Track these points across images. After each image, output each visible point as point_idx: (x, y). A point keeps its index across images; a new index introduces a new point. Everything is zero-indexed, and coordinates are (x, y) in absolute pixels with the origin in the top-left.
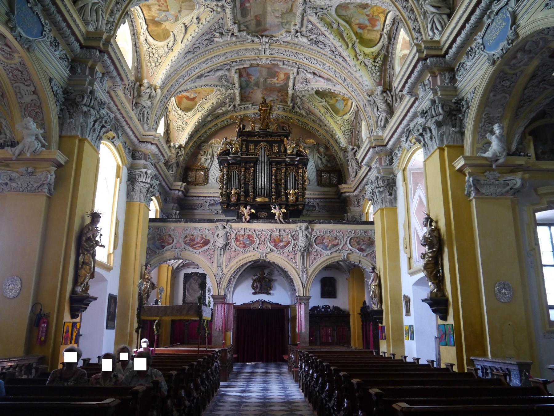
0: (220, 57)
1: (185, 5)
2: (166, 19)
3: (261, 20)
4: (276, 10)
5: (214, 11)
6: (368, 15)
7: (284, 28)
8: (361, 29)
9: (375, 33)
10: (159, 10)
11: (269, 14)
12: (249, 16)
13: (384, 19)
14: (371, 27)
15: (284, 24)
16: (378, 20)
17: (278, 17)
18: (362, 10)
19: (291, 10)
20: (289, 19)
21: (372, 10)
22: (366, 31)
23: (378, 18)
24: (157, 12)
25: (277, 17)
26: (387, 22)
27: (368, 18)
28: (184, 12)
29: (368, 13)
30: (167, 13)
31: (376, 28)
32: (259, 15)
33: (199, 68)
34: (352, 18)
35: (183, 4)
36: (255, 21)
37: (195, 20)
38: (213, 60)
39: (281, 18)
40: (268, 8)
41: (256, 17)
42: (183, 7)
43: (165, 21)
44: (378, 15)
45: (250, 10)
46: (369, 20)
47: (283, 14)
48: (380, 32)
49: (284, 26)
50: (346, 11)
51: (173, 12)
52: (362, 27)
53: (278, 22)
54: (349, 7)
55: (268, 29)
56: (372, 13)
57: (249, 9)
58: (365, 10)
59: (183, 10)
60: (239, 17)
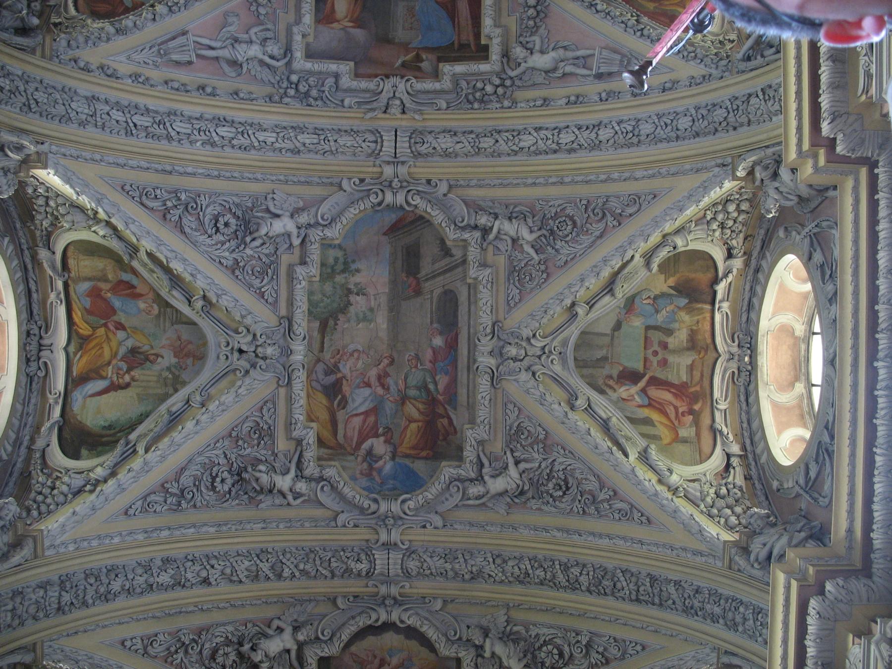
0: (532, 149)
1: (601, 347)
2: (660, 301)
3: (404, 275)
4: (365, 319)
5: (528, 339)
6: (120, 326)
7: (340, 247)
8: (127, 283)
9: (86, 272)
10: (669, 332)
11: (383, 299)
12: (437, 292)
13: (74, 316)
14: (101, 290)
15: (340, 267)
16: (89, 312)
17: (358, 294)
18: (138, 344)
19: (324, 328)
20: (328, 287)
21: (114, 344)
22: (110, 276)
23: (91, 318)
24: (676, 325)
25: (361, 292)
26: (62, 311)
27: (116, 318)
28: (605, 327)
29: (121, 335)
30: (651, 322)
31: (85, 286)
32: (409, 298)
33: (601, 138)
34: (158, 316)
35: (603, 352)
36: (423, 273)
37: (581, 311)
38: (554, 146)
39: (349, 291)
40: (385, 326)
41: (418, 292)
42: (607, 340)
43: (663, 295)
44: (94, 329)
45: (432, 323)
46: (114, 312)
47: (344, 308)
48: (73, 275)
49: (340, 254)
50: (179, 338)
51: (637, 323)
52: (126, 289)
53: (358, 271)
54: (175, 356)
55: (385, 234)
56: (111, 335)
57: (435, 325)
58: (130, 343)
59: (609, 332)
60: (463, 298)
